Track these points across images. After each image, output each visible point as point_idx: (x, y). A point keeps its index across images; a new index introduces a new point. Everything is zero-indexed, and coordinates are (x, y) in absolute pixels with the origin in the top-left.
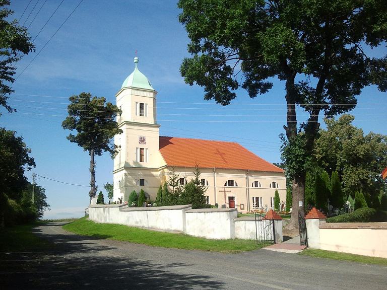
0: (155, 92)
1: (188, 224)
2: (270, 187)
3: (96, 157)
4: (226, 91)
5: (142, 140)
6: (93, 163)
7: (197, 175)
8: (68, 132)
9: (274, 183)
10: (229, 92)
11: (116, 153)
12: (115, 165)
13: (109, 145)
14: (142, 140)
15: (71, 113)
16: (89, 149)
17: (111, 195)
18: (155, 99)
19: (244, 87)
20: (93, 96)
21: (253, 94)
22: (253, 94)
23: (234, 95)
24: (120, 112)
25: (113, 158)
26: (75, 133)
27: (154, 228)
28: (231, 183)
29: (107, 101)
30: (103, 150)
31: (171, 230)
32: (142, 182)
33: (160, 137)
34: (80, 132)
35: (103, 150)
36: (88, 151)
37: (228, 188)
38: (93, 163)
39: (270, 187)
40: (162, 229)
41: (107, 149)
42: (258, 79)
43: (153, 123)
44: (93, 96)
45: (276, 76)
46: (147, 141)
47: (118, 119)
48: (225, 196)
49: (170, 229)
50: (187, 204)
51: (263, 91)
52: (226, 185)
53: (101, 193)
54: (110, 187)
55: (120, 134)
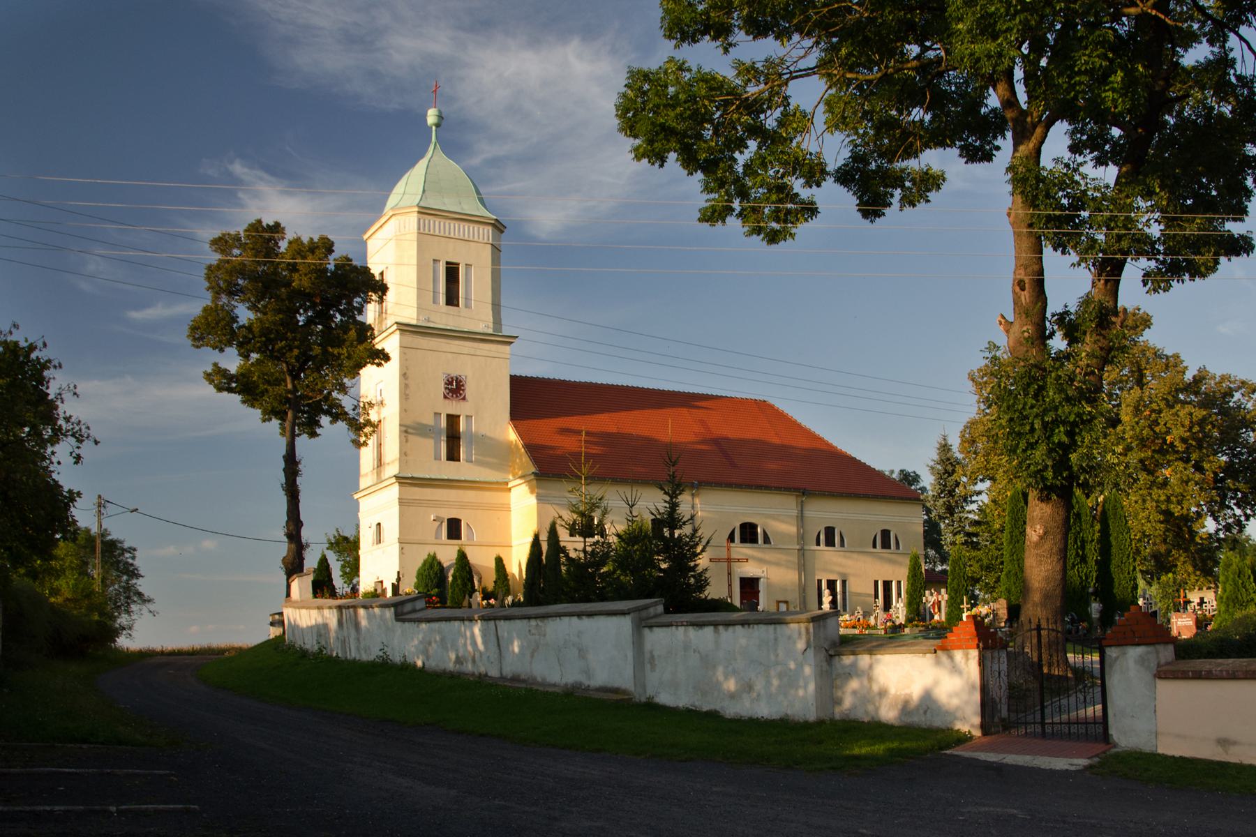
0: (498, 227)
1: (653, 667)
2: (874, 546)
3: (302, 442)
4: (782, 190)
5: (455, 388)
6: (291, 465)
7: (673, 495)
8: (209, 357)
9: (886, 534)
10: (794, 197)
11: (368, 430)
12: (363, 471)
13: (347, 402)
14: (455, 388)
15: (217, 291)
16: (281, 415)
17: (353, 569)
18: (496, 249)
19: (844, 177)
20: (290, 235)
21: (872, 207)
22: (872, 207)
23: (810, 210)
24: (381, 288)
25: (358, 445)
26: (232, 361)
27: (524, 681)
28: (748, 533)
29: (339, 251)
30: (325, 420)
31: (588, 688)
32: (454, 529)
33: (511, 376)
34: (247, 357)
35: (325, 420)
36: (275, 423)
37: (739, 550)
38: (291, 465)
39: (874, 546)
40: (555, 685)
41: (338, 414)
42: (890, 155)
43: (490, 331)
44: (290, 235)
45: (955, 151)
46: (470, 390)
47: (371, 314)
48: (729, 574)
49: (586, 683)
50: (639, 597)
51: (908, 201)
52: (731, 538)
53: (324, 563)
54: (348, 547)
55: (379, 365)
